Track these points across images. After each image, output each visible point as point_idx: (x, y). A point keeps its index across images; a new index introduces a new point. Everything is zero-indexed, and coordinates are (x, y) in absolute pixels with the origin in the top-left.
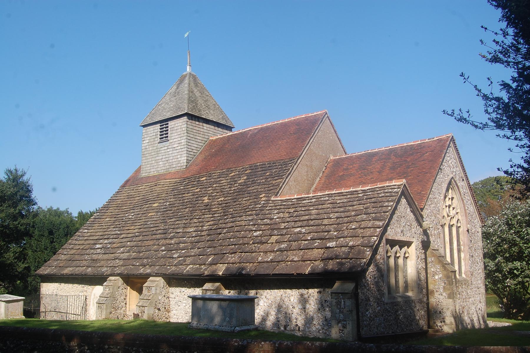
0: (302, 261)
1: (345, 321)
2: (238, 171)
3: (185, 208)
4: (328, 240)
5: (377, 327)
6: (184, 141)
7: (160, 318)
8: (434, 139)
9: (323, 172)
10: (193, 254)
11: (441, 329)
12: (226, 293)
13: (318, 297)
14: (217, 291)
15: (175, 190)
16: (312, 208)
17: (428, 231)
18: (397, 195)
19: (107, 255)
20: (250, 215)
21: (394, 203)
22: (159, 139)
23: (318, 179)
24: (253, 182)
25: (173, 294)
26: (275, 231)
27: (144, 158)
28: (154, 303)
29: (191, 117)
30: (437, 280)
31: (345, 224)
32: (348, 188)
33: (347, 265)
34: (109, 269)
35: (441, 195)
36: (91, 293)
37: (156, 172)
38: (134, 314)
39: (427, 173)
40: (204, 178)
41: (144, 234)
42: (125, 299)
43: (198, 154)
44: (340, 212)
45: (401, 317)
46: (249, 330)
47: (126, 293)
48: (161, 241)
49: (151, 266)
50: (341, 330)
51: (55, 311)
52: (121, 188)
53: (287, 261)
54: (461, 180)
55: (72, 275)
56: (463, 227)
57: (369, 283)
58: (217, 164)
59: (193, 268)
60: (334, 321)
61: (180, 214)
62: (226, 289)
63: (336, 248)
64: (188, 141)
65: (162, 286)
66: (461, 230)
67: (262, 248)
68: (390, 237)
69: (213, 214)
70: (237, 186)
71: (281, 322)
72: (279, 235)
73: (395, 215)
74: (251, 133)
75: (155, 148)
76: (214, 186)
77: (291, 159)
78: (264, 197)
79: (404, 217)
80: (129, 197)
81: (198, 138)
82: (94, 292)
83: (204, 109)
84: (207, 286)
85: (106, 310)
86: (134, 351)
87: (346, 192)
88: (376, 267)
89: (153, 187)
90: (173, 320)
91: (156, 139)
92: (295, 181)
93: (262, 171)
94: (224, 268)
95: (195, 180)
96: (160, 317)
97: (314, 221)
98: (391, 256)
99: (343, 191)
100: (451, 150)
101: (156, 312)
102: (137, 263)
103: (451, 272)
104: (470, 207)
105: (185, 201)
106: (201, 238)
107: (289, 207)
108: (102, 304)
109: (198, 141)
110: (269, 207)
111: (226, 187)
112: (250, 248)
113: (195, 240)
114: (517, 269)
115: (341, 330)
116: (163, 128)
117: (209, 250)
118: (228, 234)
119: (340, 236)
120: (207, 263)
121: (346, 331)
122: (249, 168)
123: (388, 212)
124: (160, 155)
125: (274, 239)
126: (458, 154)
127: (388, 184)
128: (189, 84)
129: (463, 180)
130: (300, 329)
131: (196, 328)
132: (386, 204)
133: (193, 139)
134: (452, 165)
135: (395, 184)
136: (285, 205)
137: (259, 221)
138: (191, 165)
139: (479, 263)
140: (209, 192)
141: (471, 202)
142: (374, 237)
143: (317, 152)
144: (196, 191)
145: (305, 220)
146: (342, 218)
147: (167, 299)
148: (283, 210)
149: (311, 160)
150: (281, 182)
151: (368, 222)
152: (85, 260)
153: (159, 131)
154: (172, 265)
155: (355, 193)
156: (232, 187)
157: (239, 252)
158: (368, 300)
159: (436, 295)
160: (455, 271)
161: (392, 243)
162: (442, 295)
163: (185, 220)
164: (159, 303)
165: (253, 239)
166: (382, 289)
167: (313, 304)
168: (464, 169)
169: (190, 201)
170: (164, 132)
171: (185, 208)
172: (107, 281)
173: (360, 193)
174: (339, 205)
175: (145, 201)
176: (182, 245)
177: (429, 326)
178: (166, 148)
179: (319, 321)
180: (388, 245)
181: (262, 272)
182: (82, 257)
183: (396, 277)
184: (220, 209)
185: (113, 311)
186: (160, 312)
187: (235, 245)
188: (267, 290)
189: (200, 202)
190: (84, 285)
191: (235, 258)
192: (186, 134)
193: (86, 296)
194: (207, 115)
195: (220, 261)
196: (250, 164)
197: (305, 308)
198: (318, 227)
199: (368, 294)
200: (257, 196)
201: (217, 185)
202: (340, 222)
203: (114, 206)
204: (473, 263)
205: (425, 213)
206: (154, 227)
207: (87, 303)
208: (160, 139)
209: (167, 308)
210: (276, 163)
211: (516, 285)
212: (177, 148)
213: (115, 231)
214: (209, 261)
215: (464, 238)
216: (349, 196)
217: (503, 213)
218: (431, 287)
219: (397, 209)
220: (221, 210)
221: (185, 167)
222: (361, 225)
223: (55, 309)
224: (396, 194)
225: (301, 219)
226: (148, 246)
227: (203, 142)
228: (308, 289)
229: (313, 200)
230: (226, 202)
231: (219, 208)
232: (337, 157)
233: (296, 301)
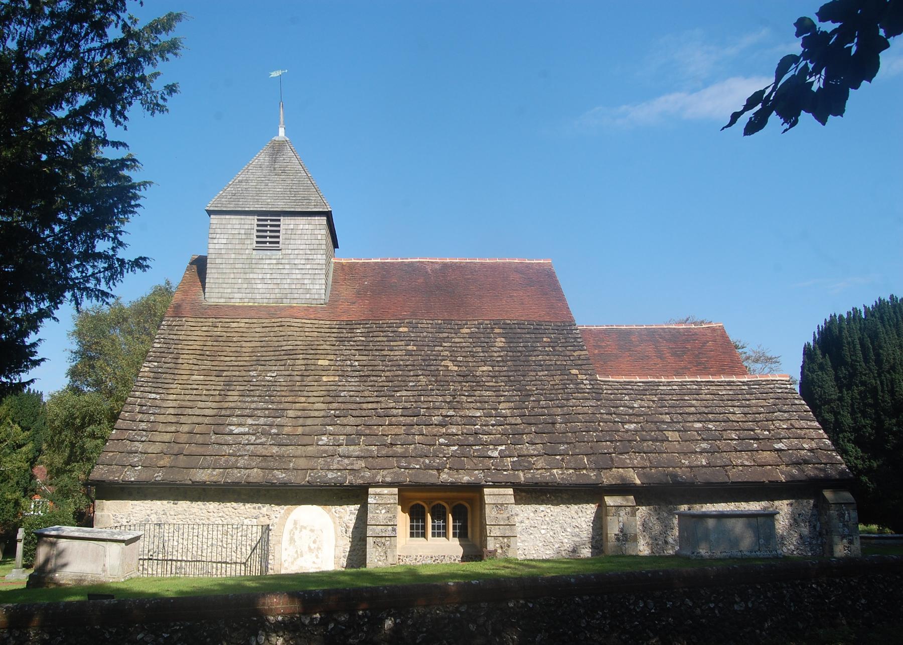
1: (851, 536)
50: (846, 547)
91: (248, 242)
108: (387, 539)
115: (846, 547)
178: (274, 262)
188: (708, 504)
190: (260, 505)
208: (257, 242)
228: (773, 500)
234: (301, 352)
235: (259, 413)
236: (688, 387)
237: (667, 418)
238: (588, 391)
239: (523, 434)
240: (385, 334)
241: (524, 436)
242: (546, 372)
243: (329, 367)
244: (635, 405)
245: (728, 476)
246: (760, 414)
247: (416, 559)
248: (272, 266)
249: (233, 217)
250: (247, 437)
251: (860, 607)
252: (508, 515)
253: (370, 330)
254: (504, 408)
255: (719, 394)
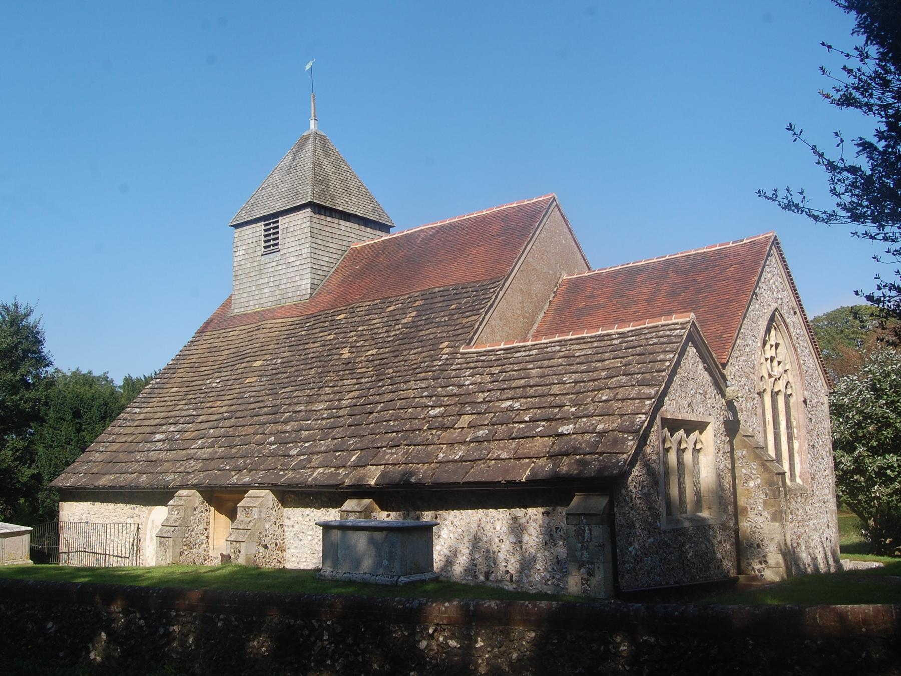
0: (514, 459)
1: (592, 563)
2: (401, 302)
3: (309, 369)
4: (561, 421)
5: (648, 574)
6: (306, 251)
7: (269, 562)
8: (743, 242)
9: (550, 301)
10: (323, 449)
11: (760, 574)
12: (383, 517)
13: (543, 522)
14: (366, 513)
15: (292, 337)
16: (531, 366)
17: (735, 404)
18: (680, 340)
19: (175, 452)
20: (424, 380)
21: (675, 355)
22: (263, 248)
23: (542, 315)
24: (428, 321)
25: (290, 519)
26: (466, 407)
27: (237, 283)
28: (257, 535)
29: (319, 209)
30: (753, 490)
31: (590, 394)
32: (593, 330)
33: (593, 465)
34: (178, 477)
35: (757, 340)
36: (147, 518)
37: (257, 306)
38: (222, 554)
39: (732, 301)
40: (342, 316)
41: (238, 414)
42: (206, 529)
43: (330, 273)
44: (581, 372)
45: (690, 554)
46: (423, 582)
47: (207, 518)
48: (268, 427)
49: (250, 471)
51: (85, 551)
52: (197, 335)
53: (488, 459)
54: (792, 312)
55: (114, 487)
56: (797, 395)
57: (634, 496)
58: (365, 291)
59: (325, 474)
60: (573, 563)
61: (300, 379)
62: (382, 511)
63: (575, 435)
64: (314, 251)
65: (271, 506)
66: (792, 400)
67: (444, 437)
68: (669, 415)
69: (359, 378)
70: (399, 329)
71: (479, 567)
72: (474, 414)
73: (678, 376)
74: (422, 235)
75: (256, 264)
76: (359, 329)
77: (493, 281)
78: (447, 347)
79: (693, 379)
80: (212, 350)
81: (331, 245)
82: (152, 517)
83: (341, 195)
84: (349, 505)
85: (173, 549)
86: (222, 620)
87: (591, 337)
88: (645, 468)
89: (254, 333)
90: (291, 565)
91: (258, 249)
92: (501, 319)
93: (443, 301)
94: (378, 473)
95: (327, 319)
96: (267, 561)
97: (534, 388)
98: (671, 447)
99: (585, 335)
100: (774, 260)
101: (261, 551)
102: (226, 465)
103: (777, 474)
104: (809, 360)
105: (310, 356)
106: (338, 421)
107: (491, 365)
108: (167, 539)
109: (332, 250)
110: (457, 364)
111: (380, 331)
112: (424, 436)
113: (327, 423)
114: (891, 467)
116: (269, 229)
117: (351, 442)
118: (386, 412)
119: (581, 414)
120: (349, 463)
121: (594, 581)
122: (421, 298)
123: (664, 371)
124: (265, 276)
125: (465, 420)
126: (786, 267)
127: (663, 322)
128: (314, 152)
129: (795, 313)
130: (514, 579)
131: (330, 578)
132: (662, 356)
133: (322, 248)
134: (776, 287)
135: (676, 321)
136: (483, 361)
137: (439, 389)
138: (319, 293)
139: (826, 459)
140: (351, 340)
141: (810, 351)
142: (640, 416)
143: (538, 267)
144: (329, 338)
145: (520, 387)
146: (584, 382)
147: (280, 528)
148: (481, 370)
149: (529, 282)
150: (476, 321)
151: (630, 390)
152: (138, 461)
153: (263, 234)
154: (287, 469)
155: (606, 338)
156: (390, 331)
157: (404, 445)
158: (632, 526)
159: (751, 515)
160: (784, 474)
161: (673, 425)
162: (761, 515)
163: (310, 389)
164: (266, 536)
165: (428, 422)
166: (656, 507)
167: (536, 535)
168: (796, 294)
169: (318, 357)
170: (272, 236)
171: (309, 369)
172: (175, 498)
173: (616, 339)
174: (578, 360)
175: (238, 358)
176: (304, 434)
177: (740, 571)
178: (275, 264)
179: (546, 563)
180: (666, 429)
181: (445, 478)
182: (131, 457)
183: (681, 484)
184: (370, 369)
185: (186, 550)
186: (268, 552)
187: (397, 432)
188: (455, 511)
189: (336, 357)
190: (134, 506)
191: (397, 454)
192: (309, 239)
193: (138, 525)
194: (346, 205)
195: (371, 460)
196: (422, 291)
197: (520, 542)
198: (543, 399)
199: (631, 515)
200: (435, 345)
201: (365, 327)
202: (580, 390)
203: (186, 366)
204: (815, 458)
205: (729, 372)
206: (256, 402)
207: (140, 536)
209: (280, 545)
210: (467, 288)
211: (891, 495)
212: (295, 264)
213: (187, 410)
214: (352, 460)
215: (798, 415)
216: (595, 344)
217: (866, 369)
218: (741, 501)
219: (680, 365)
220: (372, 371)
221: (308, 296)
222: (617, 394)
223: (84, 548)
224: (678, 339)
225: (513, 385)
226: (245, 435)
227: (340, 252)
228: (525, 507)
229: (534, 352)
230: (380, 357)
231: (369, 367)
232: (575, 276)
233: (505, 529)
248: (273, 269)
249: (248, 227)
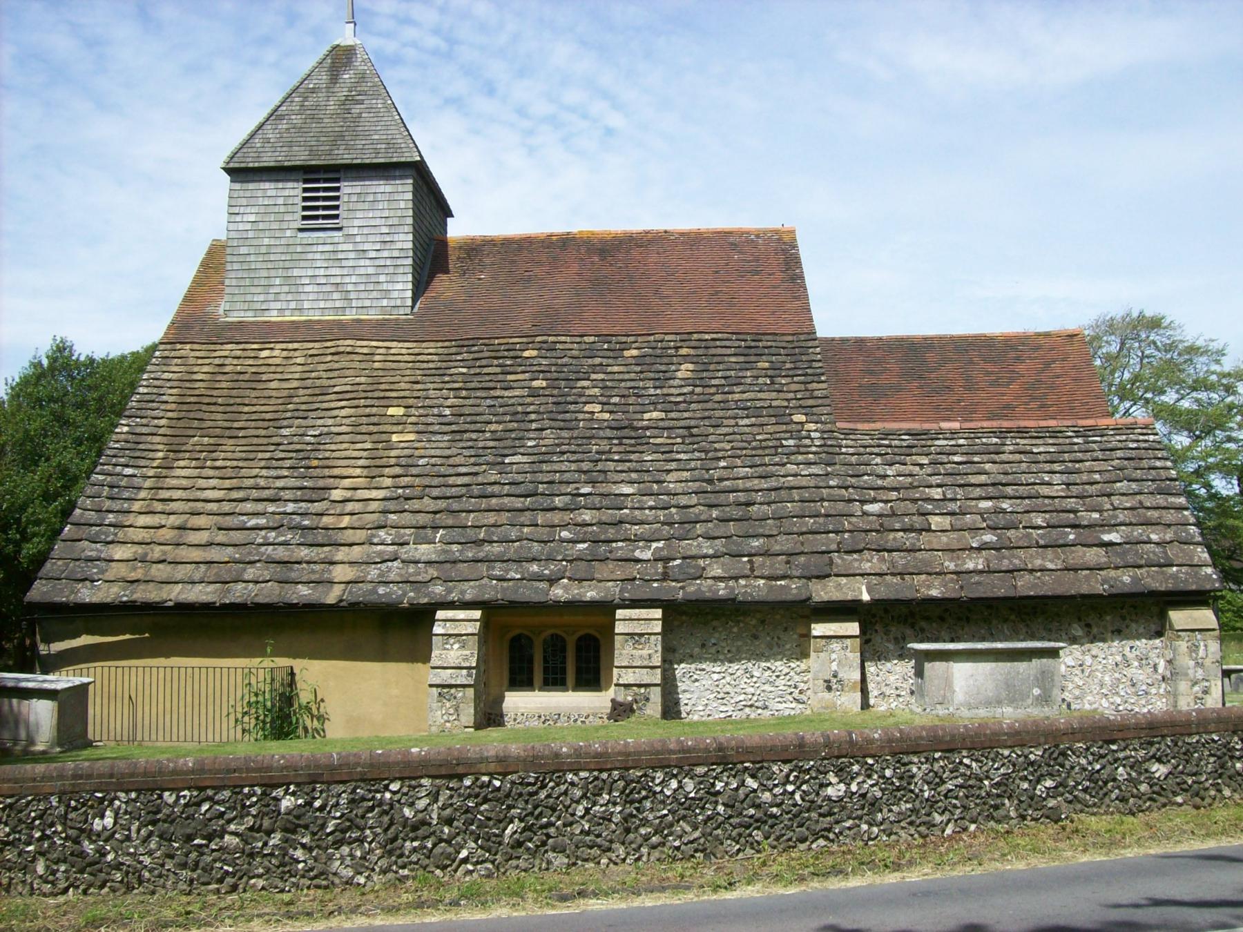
1: (1207, 681)
234: (364, 395)
235: (287, 495)
236: (984, 440)
237: (937, 493)
238: (814, 449)
239: (697, 522)
240: (501, 361)
241: (698, 526)
242: (753, 419)
243: (405, 418)
244: (889, 472)
245: (1015, 587)
246: (1092, 484)
247: (515, 720)
250: (263, 533)
251: (1043, 792)
252: (650, 651)
253: (476, 356)
254: (672, 482)
255: (1032, 453)
